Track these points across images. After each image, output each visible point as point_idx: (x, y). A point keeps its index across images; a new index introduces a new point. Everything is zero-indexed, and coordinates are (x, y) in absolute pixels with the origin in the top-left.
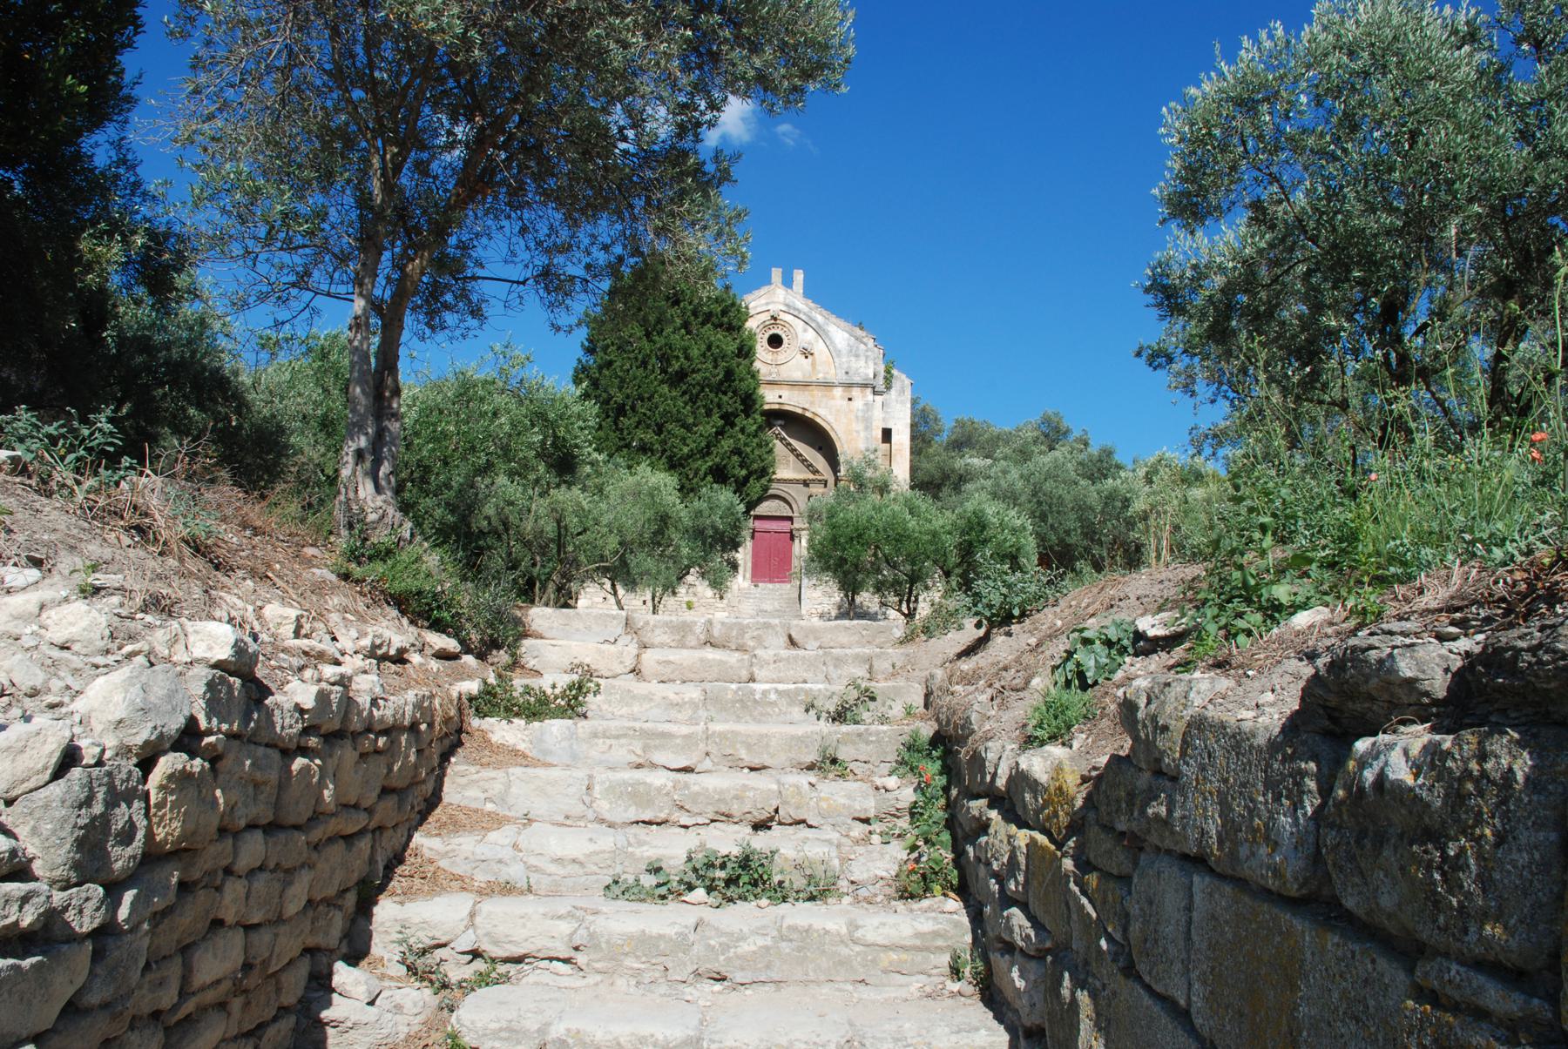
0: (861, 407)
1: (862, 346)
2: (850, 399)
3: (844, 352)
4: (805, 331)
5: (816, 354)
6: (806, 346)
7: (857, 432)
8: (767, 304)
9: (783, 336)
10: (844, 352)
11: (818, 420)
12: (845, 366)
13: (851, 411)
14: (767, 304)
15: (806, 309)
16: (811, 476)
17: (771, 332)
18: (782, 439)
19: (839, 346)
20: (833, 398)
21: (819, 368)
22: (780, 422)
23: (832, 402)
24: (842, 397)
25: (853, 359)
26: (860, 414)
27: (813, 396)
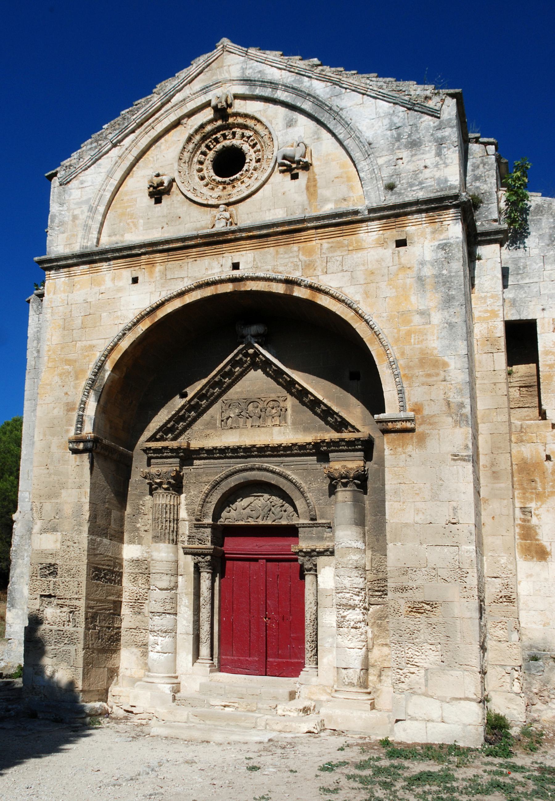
0: (429, 256)
6: (289, 151)
8: (205, 89)
13: (404, 268)
14: (205, 89)
15: (287, 77)
16: (331, 435)
17: (219, 147)
18: (266, 365)
22: (254, 329)
23: (357, 256)
26: (428, 271)
27: (310, 252)
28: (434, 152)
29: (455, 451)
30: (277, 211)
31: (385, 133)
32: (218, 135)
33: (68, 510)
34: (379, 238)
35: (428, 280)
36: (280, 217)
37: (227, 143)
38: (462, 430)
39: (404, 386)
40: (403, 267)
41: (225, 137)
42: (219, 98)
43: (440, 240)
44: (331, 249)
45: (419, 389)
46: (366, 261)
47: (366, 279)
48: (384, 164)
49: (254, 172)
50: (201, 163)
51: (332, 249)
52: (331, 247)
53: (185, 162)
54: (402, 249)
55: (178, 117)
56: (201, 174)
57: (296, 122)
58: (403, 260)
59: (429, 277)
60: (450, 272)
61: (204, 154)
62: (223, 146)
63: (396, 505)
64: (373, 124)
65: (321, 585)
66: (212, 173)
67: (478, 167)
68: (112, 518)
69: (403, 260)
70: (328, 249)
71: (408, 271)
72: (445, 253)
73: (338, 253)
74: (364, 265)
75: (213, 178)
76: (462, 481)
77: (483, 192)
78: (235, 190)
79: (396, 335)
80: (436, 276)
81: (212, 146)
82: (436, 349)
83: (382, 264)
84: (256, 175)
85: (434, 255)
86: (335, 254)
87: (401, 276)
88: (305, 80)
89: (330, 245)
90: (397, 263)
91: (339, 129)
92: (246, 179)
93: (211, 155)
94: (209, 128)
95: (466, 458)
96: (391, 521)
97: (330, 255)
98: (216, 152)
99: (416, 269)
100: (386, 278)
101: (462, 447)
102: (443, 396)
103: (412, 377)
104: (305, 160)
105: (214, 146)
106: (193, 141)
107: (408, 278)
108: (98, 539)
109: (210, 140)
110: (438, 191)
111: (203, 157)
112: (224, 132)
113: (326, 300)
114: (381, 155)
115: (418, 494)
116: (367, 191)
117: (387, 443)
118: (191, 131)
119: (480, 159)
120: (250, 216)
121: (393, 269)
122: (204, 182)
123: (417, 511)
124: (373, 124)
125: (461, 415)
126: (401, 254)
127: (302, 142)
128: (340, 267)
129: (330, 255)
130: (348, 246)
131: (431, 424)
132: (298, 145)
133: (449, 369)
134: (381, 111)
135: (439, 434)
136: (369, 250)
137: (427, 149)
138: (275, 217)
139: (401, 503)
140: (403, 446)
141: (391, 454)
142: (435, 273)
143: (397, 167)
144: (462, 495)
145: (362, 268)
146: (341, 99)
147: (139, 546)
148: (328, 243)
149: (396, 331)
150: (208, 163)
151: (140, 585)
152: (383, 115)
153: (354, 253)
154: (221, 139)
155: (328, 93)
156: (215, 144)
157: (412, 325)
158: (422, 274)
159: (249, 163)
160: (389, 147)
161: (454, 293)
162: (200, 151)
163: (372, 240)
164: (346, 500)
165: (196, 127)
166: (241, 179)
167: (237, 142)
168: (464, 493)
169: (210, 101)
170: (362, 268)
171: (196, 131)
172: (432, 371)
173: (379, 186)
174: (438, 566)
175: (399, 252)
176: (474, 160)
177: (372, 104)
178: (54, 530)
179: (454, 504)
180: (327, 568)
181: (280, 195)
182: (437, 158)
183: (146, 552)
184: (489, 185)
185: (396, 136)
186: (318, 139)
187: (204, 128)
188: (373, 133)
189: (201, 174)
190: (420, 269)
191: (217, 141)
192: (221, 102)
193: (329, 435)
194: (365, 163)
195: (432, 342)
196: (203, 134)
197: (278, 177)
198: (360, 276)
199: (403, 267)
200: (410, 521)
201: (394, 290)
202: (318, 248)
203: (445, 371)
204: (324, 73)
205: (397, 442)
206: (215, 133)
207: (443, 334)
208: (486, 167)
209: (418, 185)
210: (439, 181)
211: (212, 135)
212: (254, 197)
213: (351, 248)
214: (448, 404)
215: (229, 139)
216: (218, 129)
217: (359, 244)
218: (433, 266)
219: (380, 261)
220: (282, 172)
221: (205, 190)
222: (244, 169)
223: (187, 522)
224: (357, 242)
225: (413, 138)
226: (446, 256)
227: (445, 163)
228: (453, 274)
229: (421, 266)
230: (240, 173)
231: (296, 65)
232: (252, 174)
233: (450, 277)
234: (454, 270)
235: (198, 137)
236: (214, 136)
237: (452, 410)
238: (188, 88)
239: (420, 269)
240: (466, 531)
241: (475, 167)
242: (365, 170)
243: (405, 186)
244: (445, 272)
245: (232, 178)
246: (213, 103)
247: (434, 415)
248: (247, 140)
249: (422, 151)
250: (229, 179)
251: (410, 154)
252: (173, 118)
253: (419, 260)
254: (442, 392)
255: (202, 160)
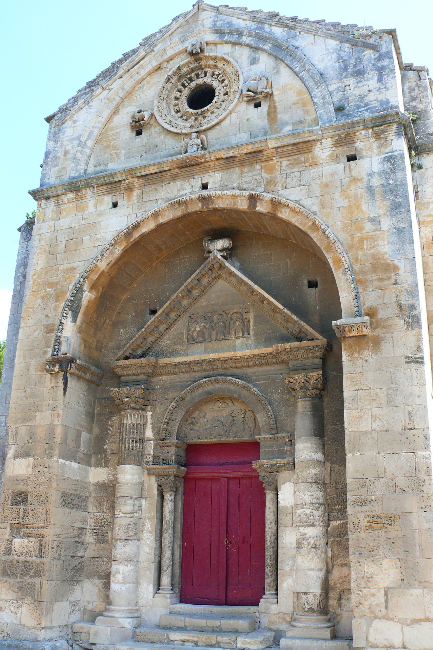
1: (369, 54)
2: (352, 158)
3: (331, 73)
4: (254, 62)
5: (275, 93)
7: (374, 220)
9: (215, 84)
10: (331, 73)
11: (284, 214)
12: (336, 98)
13: (354, 180)
17: (193, 84)
19: (321, 66)
20: (315, 164)
21: (282, 116)
23: (314, 172)
24: (335, 159)
25: (351, 81)
26: (376, 182)
27: (270, 170)
28: (376, 79)
29: (408, 353)
30: (242, 135)
31: (334, 65)
32: (193, 75)
33: (41, 433)
34: (332, 154)
35: (377, 189)
36: (244, 140)
37: (200, 81)
38: (414, 332)
39: (359, 291)
40: (354, 179)
41: (198, 76)
42: (194, 45)
43: (386, 153)
44: (290, 166)
45: (373, 293)
46: (321, 175)
47: (321, 192)
48: (334, 91)
49: (222, 103)
50: (177, 99)
51: (290, 166)
52: (290, 164)
53: (163, 99)
54: (352, 163)
55: (159, 63)
56: (177, 108)
57: (258, 60)
58: (354, 173)
59: (377, 187)
60: (396, 181)
61: (180, 91)
62: (197, 84)
63: (354, 413)
64: (323, 59)
65: (282, 503)
66: (186, 106)
67: (414, 90)
68: (82, 440)
69: (354, 173)
70: (287, 166)
71: (359, 183)
72: (391, 165)
73: (297, 169)
74: (319, 179)
75: (187, 110)
76: (416, 384)
77: (419, 110)
78: (206, 120)
79: (350, 242)
80: (383, 186)
81: (187, 84)
82: (387, 253)
83: (336, 177)
84: (224, 105)
85: (381, 166)
86: (294, 170)
87: (352, 187)
88: (266, 27)
89: (289, 162)
90: (349, 175)
91: (295, 64)
92: (215, 110)
93: (186, 92)
94: (185, 70)
95: (419, 360)
96: (350, 430)
97: (290, 171)
98: (191, 88)
99: (365, 180)
100: (339, 190)
101: (415, 349)
102: (394, 299)
103: (366, 282)
104: (266, 91)
105: (189, 84)
106: (170, 81)
107: (359, 188)
108: (67, 463)
109: (185, 79)
110: (381, 111)
111: (179, 93)
112: (198, 72)
113: (286, 213)
114: (331, 83)
115: (374, 400)
116: (320, 114)
117: (345, 348)
118: (170, 73)
119: (415, 83)
120: (218, 140)
121: (346, 181)
122: (179, 115)
123: (375, 418)
124: (323, 59)
125: (413, 317)
126: (352, 167)
127: (264, 77)
128: (298, 181)
129: (290, 171)
130: (305, 162)
131: (385, 328)
132: (261, 79)
133: (400, 272)
134: (330, 48)
135: (392, 337)
136: (324, 165)
137: (370, 76)
138: (240, 140)
139: (359, 411)
140: (359, 352)
141: (348, 361)
142: (382, 183)
143: (345, 92)
144: (417, 398)
145: (318, 181)
146: (296, 40)
147: (106, 469)
148: (288, 161)
149: (349, 238)
150: (184, 100)
151: (105, 510)
152: (332, 51)
153: (310, 168)
154: (195, 78)
155: (285, 36)
156: (189, 82)
157: (364, 231)
158: (371, 184)
159: (218, 95)
160: (338, 76)
161: (400, 200)
162: (176, 89)
163: (326, 156)
164: (306, 410)
165: (174, 69)
166: (210, 110)
167: (208, 80)
168: (418, 396)
169: (187, 47)
170: (318, 181)
171: (174, 74)
172: (384, 276)
173: (331, 109)
174: (396, 475)
175: (350, 166)
176: (410, 84)
177: (322, 43)
178: (27, 454)
179: (410, 408)
180: (287, 484)
181: (244, 121)
182: (379, 84)
183: (112, 475)
184: (424, 104)
185: (343, 67)
186: (277, 72)
187: (180, 70)
188: (324, 65)
189: (177, 108)
190: (369, 180)
191: (191, 80)
192: (196, 48)
193: (289, 344)
194: (318, 91)
195: (383, 247)
196: (180, 75)
197: (244, 106)
198: (316, 189)
199: (354, 179)
200: (368, 428)
201: (347, 200)
202: (278, 166)
203: (396, 275)
204: (281, 21)
205: (354, 348)
206: (190, 73)
207: (392, 239)
208: (421, 89)
209: (364, 107)
210: (381, 103)
211: (187, 75)
212: (223, 124)
213: (307, 164)
214: (400, 307)
215: (202, 77)
216: (193, 70)
217: (315, 160)
218: (380, 177)
219: (333, 174)
220: (248, 101)
221: (180, 122)
222: (214, 101)
223: (152, 442)
224: (313, 158)
225: (358, 68)
226: (391, 167)
227: (386, 87)
228: (398, 183)
229: (370, 177)
230: (210, 105)
231: (258, 16)
232: (221, 105)
233: (396, 186)
234: (399, 180)
235: (175, 78)
236: (189, 76)
237: (404, 313)
238: (168, 39)
239: (369, 180)
240: (421, 436)
241: (410, 90)
242: (318, 96)
243: (353, 108)
244: (391, 182)
245: (203, 109)
246: (189, 49)
247: (388, 318)
248: (216, 77)
249: (365, 78)
250: (200, 110)
251: (356, 81)
252: (155, 64)
253: (368, 172)
254: (394, 295)
255: (178, 96)
